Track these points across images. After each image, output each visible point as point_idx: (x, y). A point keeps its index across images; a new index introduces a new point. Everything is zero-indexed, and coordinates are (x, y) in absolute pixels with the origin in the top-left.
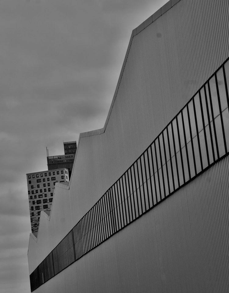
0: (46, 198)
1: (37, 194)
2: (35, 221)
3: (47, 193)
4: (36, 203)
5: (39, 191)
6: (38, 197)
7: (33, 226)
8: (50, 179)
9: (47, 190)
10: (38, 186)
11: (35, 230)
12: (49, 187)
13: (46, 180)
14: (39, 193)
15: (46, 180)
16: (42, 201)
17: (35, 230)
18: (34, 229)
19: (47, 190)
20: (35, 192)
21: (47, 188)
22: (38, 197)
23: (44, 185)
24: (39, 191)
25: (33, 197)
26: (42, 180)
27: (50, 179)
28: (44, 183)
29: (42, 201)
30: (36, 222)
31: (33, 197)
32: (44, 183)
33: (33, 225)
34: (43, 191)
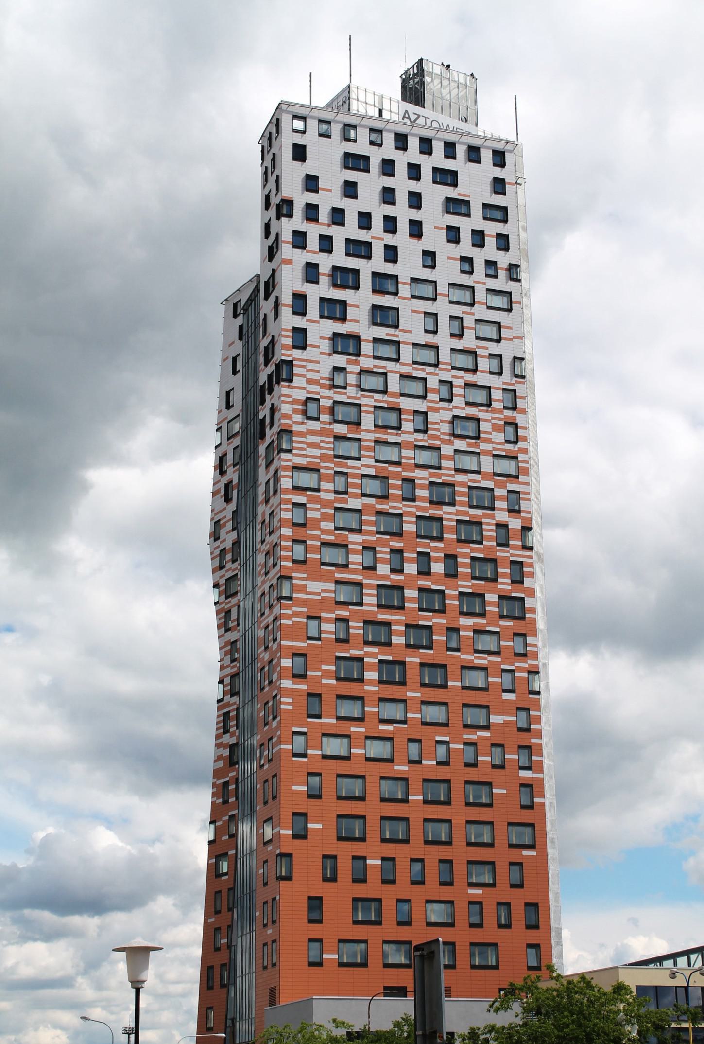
0: (388, 268)
1: (340, 235)
2: (310, 381)
3: (402, 238)
4: (324, 280)
5: (351, 219)
6: (339, 246)
7: (295, 411)
8: (426, 173)
9: (403, 227)
10: (350, 190)
11: (303, 435)
12: (415, 215)
13: (401, 170)
14: (351, 229)
15: (401, 170)
16: (366, 280)
17: (303, 435)
18: (296, 428)
19: (403, 227)
20: (324, 215)
21: (403, 212)
22: (339, 246)
23: (388, 196)
24: (351, 219)
25: (313, 242)
26: (375, 164)
27: (426, 173)
28: (388, 182)
29: (366, 280)
30: (316, 388)
31: (313, 242)
32: (388, 182)
33: (295, 402)
34: (378, 223)
